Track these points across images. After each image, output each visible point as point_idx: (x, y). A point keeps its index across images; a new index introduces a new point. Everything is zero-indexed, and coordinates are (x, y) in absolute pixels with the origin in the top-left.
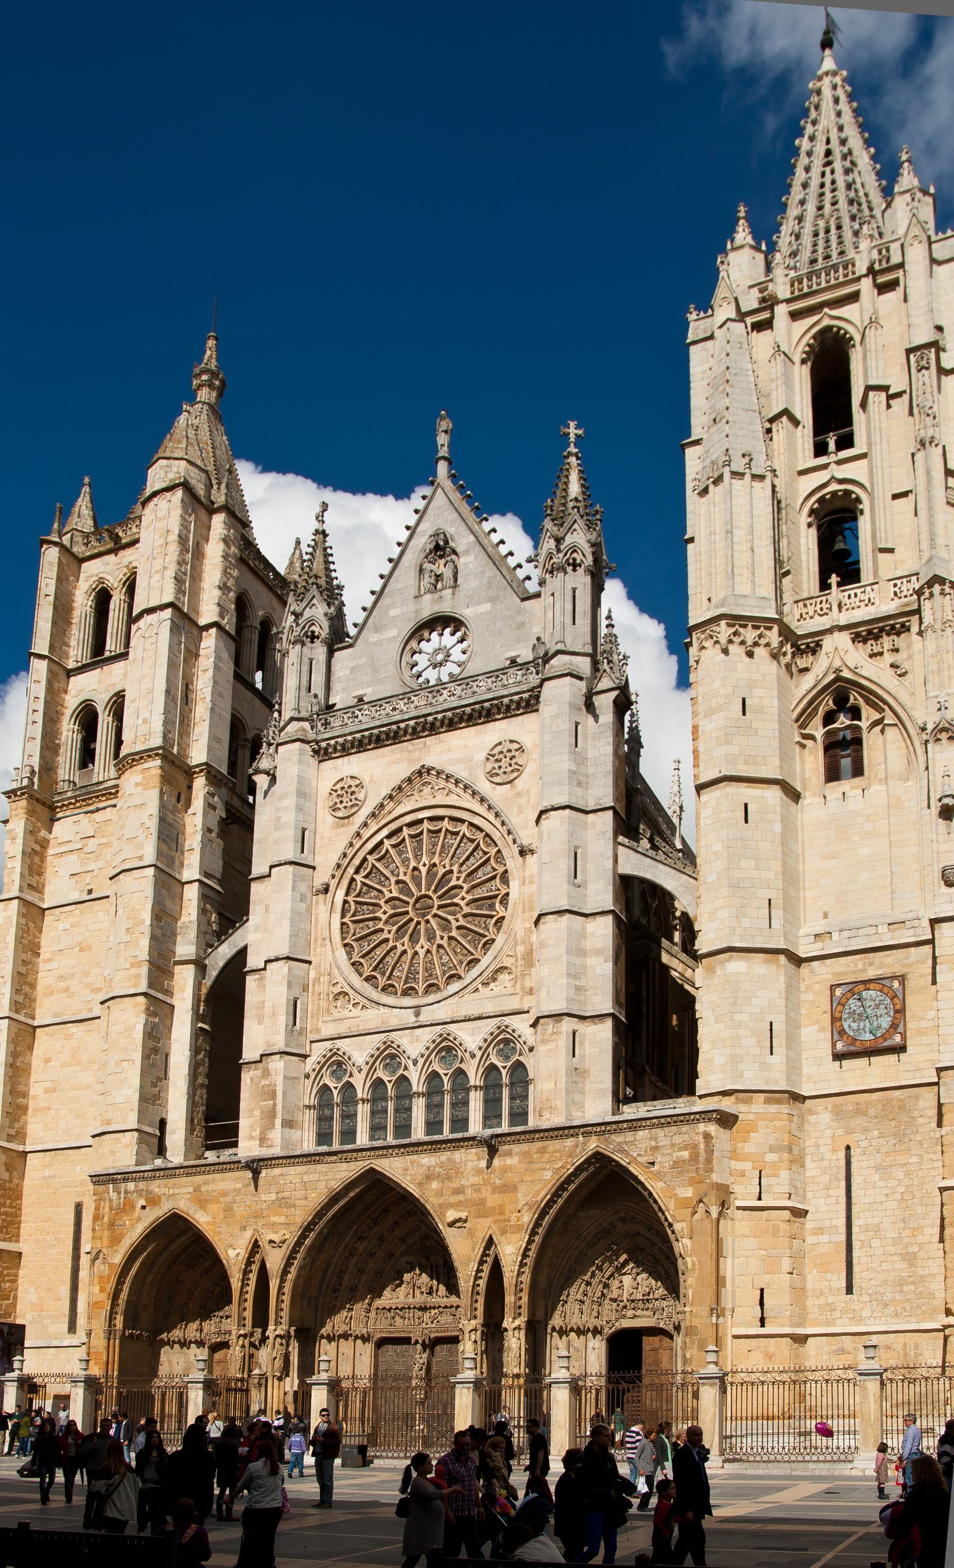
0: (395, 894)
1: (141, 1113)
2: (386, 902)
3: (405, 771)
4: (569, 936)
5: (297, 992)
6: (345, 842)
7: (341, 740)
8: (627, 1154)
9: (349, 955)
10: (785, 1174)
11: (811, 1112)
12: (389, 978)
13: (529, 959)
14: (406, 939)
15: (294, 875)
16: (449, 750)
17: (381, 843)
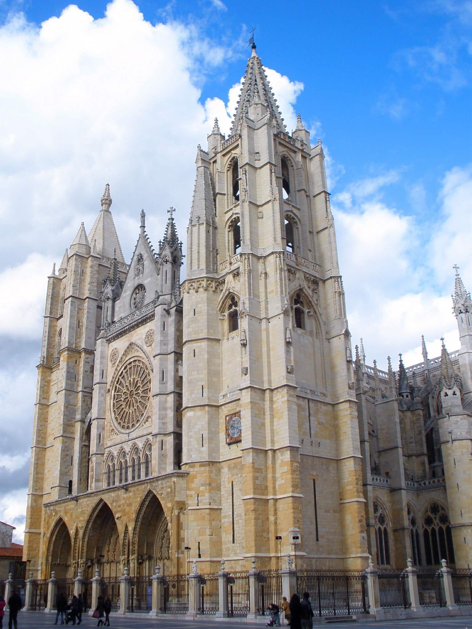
0: (125, 391)
1: (60, 479)
2: (124, 394)
3: (127, 344)
4: (160, 404)
5: (100, 430)
6: (113, 374)
7: (112, 336)
8: (156, 491)
9: (115, 414)
10: (207, 495)
11: (223, 468)
12: (124, 422)
13: (152, 411)
14: (128, 407)
15: (99, 388)
16: (137, 335)
17: (122, 372)
